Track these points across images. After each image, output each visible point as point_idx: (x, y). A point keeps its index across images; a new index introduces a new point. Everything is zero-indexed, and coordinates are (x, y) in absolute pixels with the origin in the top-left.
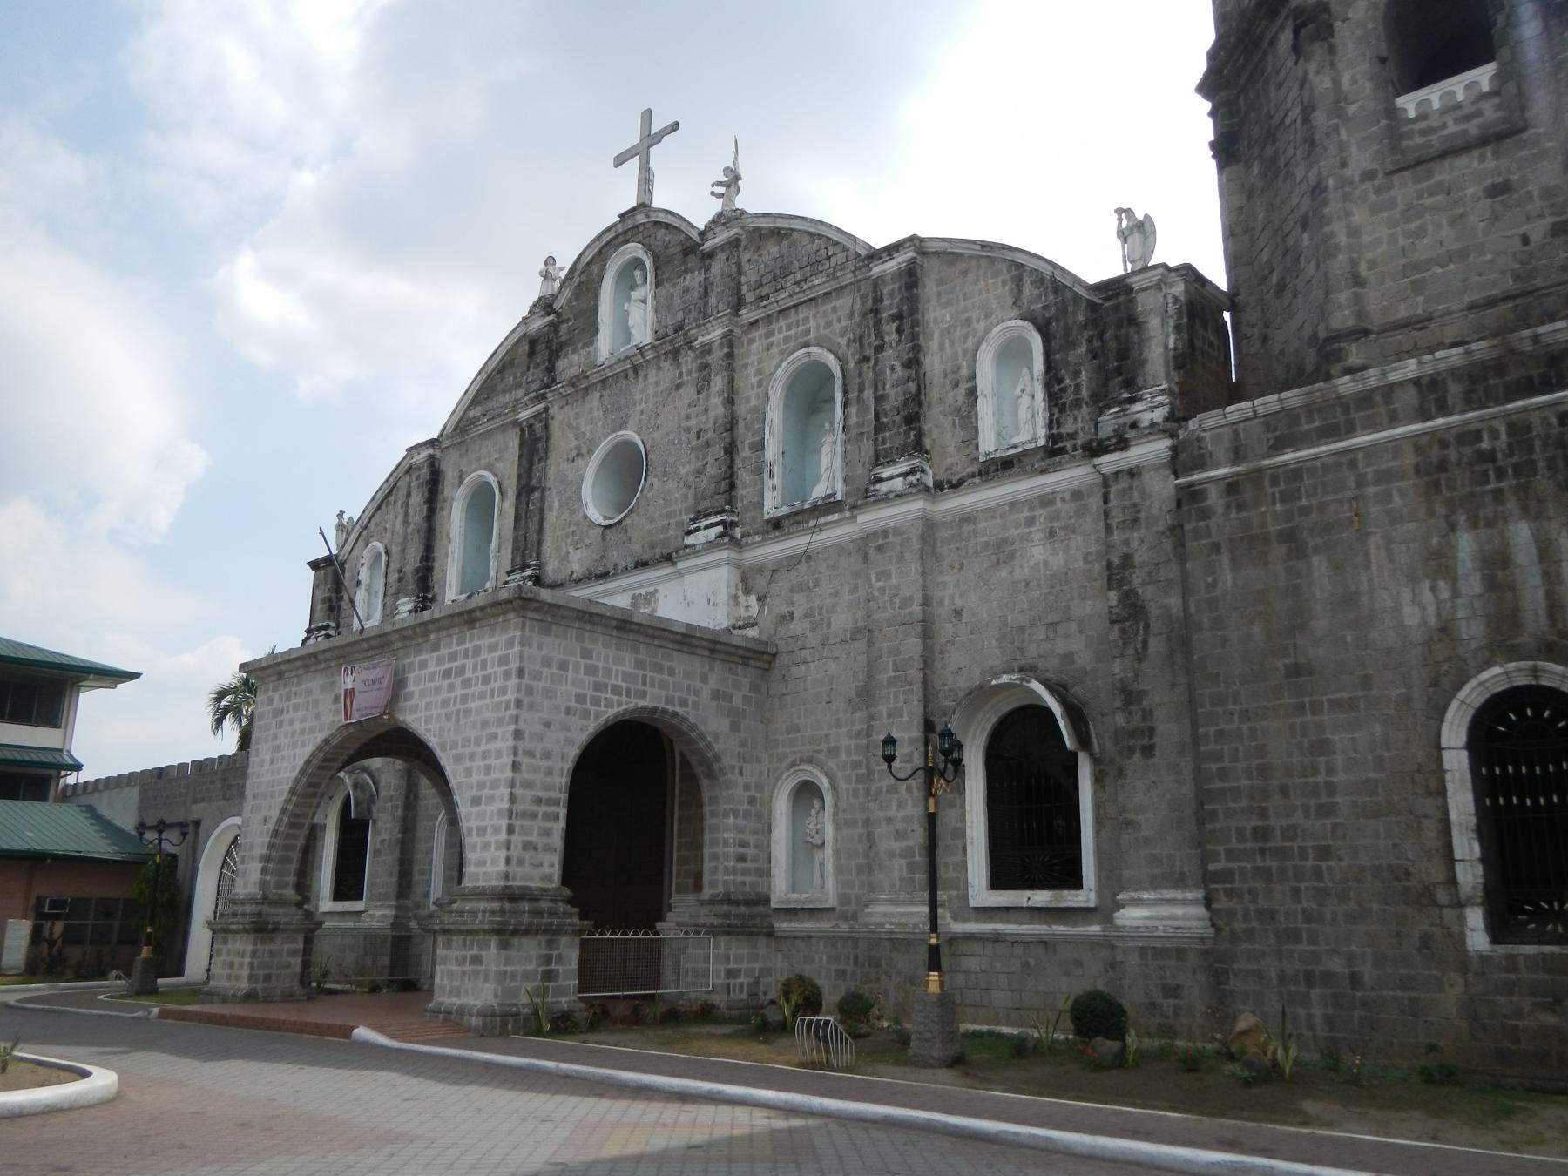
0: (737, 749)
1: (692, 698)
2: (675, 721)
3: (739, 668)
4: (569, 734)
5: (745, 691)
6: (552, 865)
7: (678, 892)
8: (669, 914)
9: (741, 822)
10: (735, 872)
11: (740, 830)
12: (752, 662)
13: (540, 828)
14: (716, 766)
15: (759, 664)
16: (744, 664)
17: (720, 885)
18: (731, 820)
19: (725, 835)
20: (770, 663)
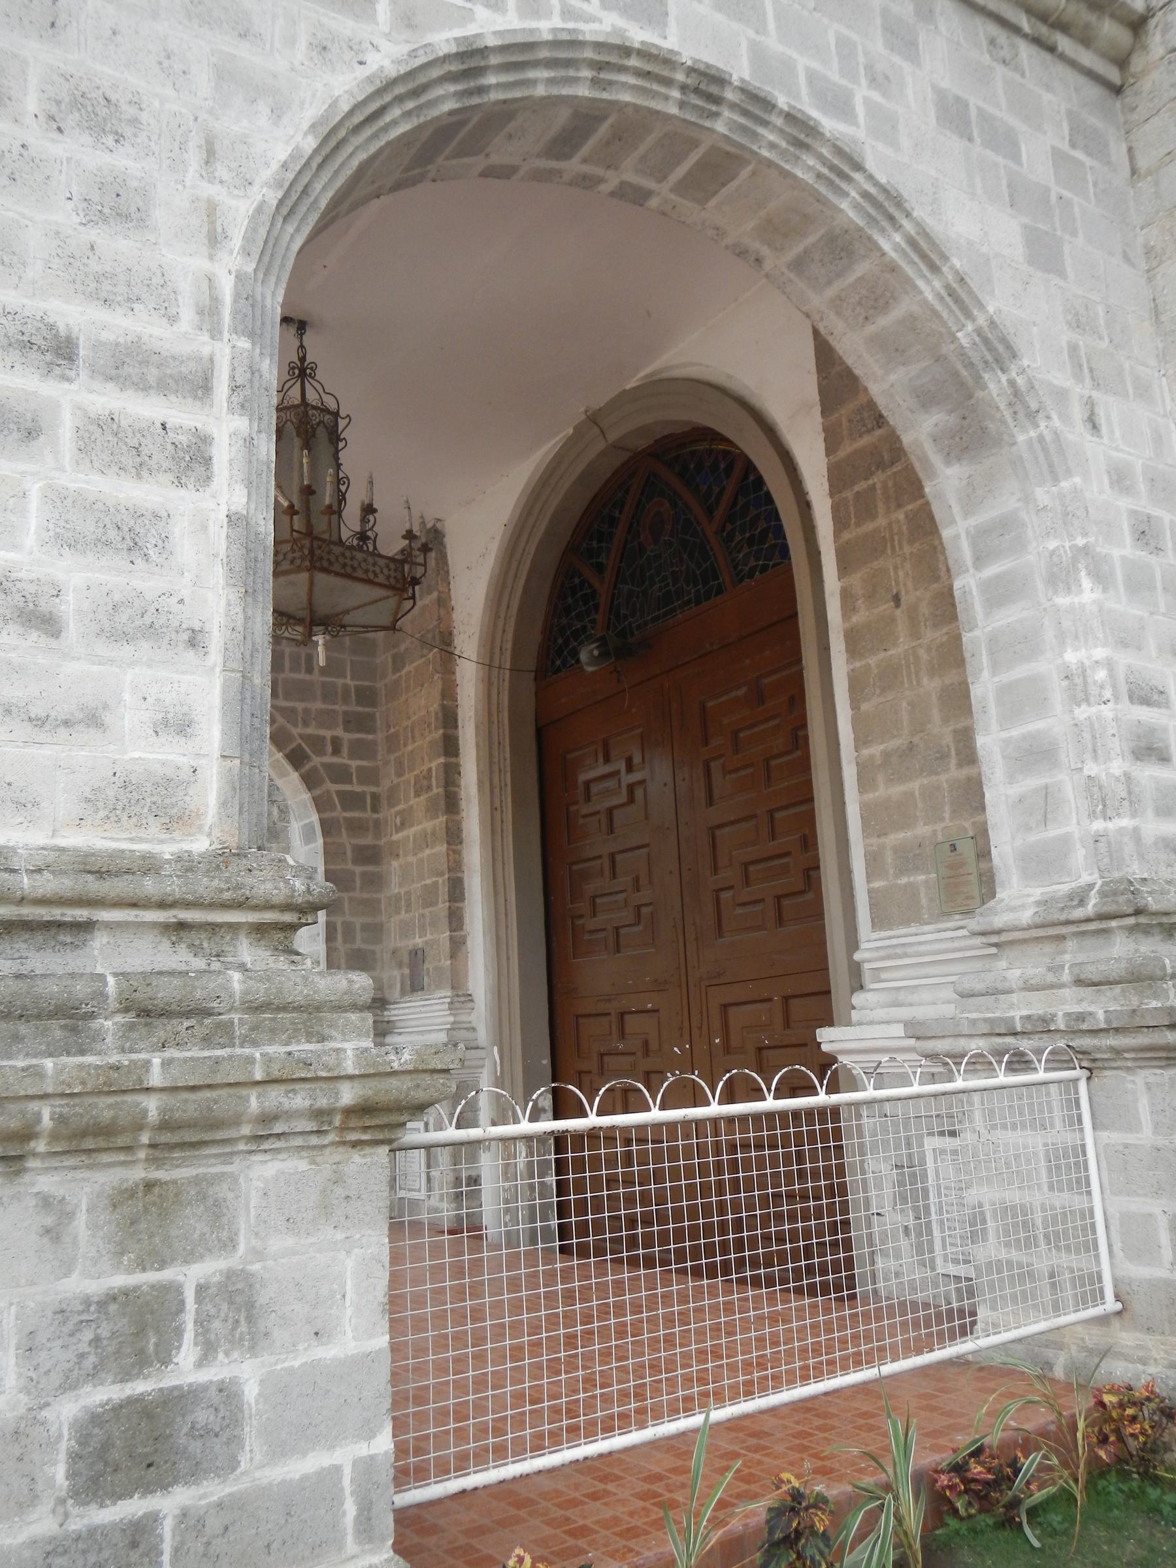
0: (1066, 336)
1: (862, 93)
2: (805, 169)
3: (1025, 51)
4: (245, 53)
5: (1055, 136)
6: (183, 727)
7: (879, 922)
8: (858, 999)
9: (1121, 605)
10: (1132, 800)
11: (1127, 639)
12: (1064, 43)
13: (57, 497)
14: (995, 386)
15: (1087, 58)
16: (1037, 41)
17: (1079, 856)
18: (1088, 593)
19: (1072, 657)
20: (1122, 63)
